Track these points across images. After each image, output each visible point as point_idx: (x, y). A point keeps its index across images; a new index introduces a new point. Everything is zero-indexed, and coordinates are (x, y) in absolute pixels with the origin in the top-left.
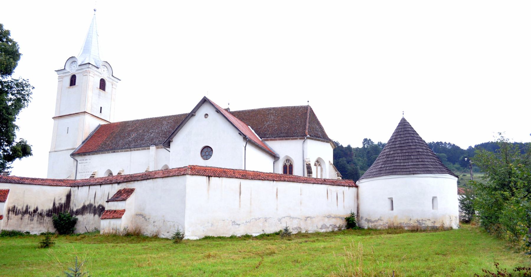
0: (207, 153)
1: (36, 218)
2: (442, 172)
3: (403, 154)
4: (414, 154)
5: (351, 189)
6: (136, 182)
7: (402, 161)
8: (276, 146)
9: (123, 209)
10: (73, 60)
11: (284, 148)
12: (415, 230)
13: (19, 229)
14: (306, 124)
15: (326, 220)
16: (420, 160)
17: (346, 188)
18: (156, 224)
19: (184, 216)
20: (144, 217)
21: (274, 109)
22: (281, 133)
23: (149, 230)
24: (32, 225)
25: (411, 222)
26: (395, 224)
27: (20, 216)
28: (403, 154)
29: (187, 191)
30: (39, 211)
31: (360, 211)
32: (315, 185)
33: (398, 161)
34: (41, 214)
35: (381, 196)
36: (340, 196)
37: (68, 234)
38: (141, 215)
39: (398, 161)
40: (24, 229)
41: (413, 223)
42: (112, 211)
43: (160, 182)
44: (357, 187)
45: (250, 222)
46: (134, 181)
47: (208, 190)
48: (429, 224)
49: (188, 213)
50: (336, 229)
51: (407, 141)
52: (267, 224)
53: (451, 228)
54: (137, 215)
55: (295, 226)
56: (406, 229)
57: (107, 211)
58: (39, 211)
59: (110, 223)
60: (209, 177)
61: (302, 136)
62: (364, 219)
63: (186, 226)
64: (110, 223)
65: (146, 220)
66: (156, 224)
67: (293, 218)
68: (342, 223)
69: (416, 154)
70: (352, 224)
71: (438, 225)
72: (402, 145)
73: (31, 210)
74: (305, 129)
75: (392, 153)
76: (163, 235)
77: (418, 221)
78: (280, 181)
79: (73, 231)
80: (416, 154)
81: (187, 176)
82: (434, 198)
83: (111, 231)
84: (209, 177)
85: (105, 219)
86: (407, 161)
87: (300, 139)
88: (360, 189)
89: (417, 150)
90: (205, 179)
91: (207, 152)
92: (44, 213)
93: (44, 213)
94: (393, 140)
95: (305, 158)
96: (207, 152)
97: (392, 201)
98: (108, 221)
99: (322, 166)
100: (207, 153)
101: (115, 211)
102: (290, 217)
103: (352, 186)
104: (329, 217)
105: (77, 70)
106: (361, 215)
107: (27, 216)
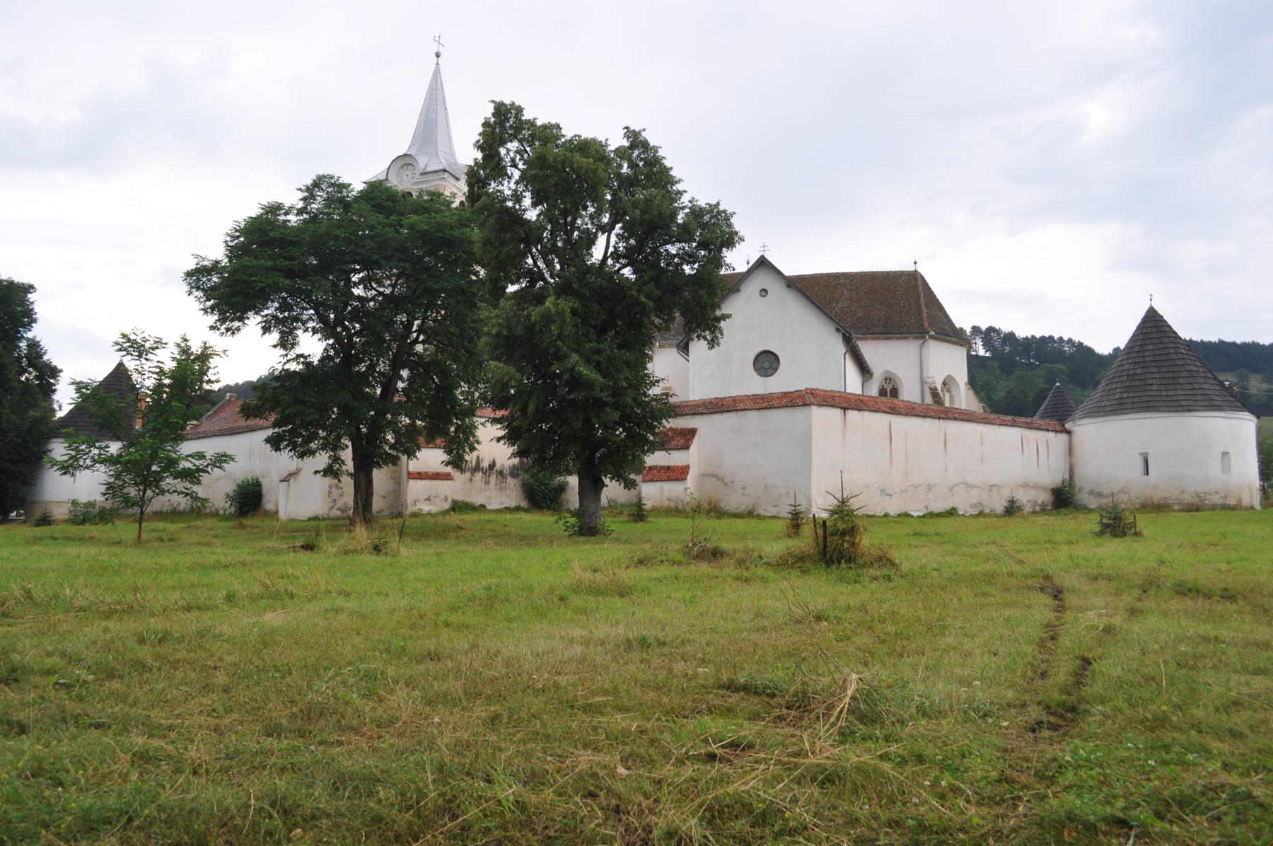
0: (767, 365)
1: (493, 479)
2: (1236, 409)
3: (1162, 375)
4: (1182, 374)
5: (1059, 435)
6: (698, 417)
7: (1162, 387)
8: (871, 350)
9: (684, 464)
10: (407, 160)
11: (879, 354)
12: (1193, 508)
13: (469, 500)
14: (920, 310)
15: (1022, 491)
16: (1196, 386)
17: (1052, 435)
18: (747, 491)
19: (809, 478)
20: (722, 480)
21: (846, 275)
22: (874, 325)
23: (734, 502)
24: (488, 493)
25: (1185, 496)
26: (1156, 501)
27: (468, 475)
28: (1162, 375)
29: (815, 432)
30: (498, 467)
31: (1076, 478)
32: (1003, 428)
33: (1155, 387)
34: (501, 473)
35: (1112, 448)
36: (1042, 448)
37: (548, 508)
38: (712, 475)
39: (1155, 387)
40: (477, 500)
41: (1187, 498)
42: (662, 467)
43: (753, 417)
44: (1069, 432)
45: (905, 491)
46: (694, 414)
47: (844, 433)
48: (1216, 499)
49: (815, 472)
50: (1038, 509)
51: (1166, 351)
52: (931, 496)
53: (1253, 508)
54: (703, 475)
55: (974, 501)
56: (1176, 507)
57: (651, 468)
58: (498, 467)
59: (662, 489)
60: (845, 409)
61: (919, 333)
62: (1087, 490)
63: (814, 494)
64: (662, 489)
65: (726, 484)
66: (747, 491)
67: (972, 486)
68: (1045, 497)
69: (1186, 374)
70: (1063, 499)
71: (1232, 502)
72: (1159, 358)
73: (485, 464)
74: (922, 319)
75: (1139, 371)
76: (765, 509)
77: (1197, 495)
78: (949, 419)
79: (561, 505)
80: (1186, 374)
81: (814, 408)
82: (1225, 454)
83: (666, 503)
84: (845, 409)
85: (651, 481)
86: (1171, 387)
87: (915, 338)
88: (1076, 438)
89: (1188, 368)
90: (837, 412)
91: (767, 362)
92: (507, 471)
93: (507, 471)
94: (1137, 349)
95: (925, 375)
96: (767, 362)
97: (1146, 461)
98: (658, 484)
99: (954, 392)
100: (767, 365)
101: (668, 468)
102: (966, 484)
103: (1061, 432)
104: (1026, 486)
105: (416, 183)
106: (1078, 483)
107: (479, 475)
